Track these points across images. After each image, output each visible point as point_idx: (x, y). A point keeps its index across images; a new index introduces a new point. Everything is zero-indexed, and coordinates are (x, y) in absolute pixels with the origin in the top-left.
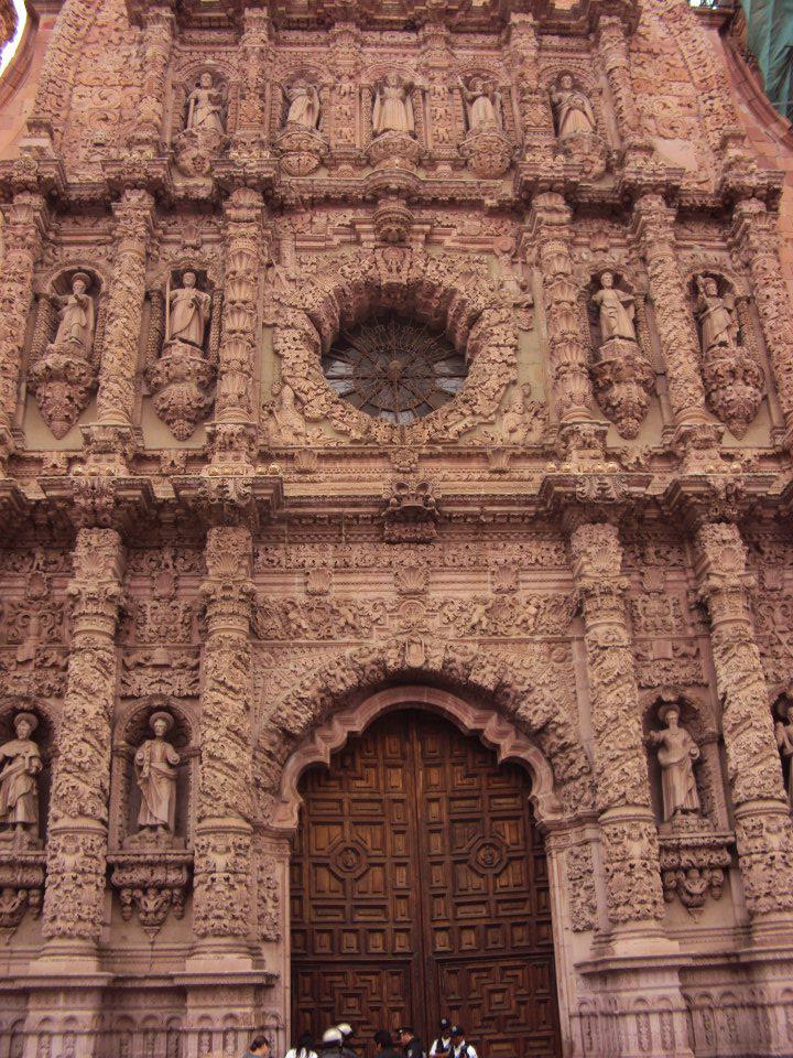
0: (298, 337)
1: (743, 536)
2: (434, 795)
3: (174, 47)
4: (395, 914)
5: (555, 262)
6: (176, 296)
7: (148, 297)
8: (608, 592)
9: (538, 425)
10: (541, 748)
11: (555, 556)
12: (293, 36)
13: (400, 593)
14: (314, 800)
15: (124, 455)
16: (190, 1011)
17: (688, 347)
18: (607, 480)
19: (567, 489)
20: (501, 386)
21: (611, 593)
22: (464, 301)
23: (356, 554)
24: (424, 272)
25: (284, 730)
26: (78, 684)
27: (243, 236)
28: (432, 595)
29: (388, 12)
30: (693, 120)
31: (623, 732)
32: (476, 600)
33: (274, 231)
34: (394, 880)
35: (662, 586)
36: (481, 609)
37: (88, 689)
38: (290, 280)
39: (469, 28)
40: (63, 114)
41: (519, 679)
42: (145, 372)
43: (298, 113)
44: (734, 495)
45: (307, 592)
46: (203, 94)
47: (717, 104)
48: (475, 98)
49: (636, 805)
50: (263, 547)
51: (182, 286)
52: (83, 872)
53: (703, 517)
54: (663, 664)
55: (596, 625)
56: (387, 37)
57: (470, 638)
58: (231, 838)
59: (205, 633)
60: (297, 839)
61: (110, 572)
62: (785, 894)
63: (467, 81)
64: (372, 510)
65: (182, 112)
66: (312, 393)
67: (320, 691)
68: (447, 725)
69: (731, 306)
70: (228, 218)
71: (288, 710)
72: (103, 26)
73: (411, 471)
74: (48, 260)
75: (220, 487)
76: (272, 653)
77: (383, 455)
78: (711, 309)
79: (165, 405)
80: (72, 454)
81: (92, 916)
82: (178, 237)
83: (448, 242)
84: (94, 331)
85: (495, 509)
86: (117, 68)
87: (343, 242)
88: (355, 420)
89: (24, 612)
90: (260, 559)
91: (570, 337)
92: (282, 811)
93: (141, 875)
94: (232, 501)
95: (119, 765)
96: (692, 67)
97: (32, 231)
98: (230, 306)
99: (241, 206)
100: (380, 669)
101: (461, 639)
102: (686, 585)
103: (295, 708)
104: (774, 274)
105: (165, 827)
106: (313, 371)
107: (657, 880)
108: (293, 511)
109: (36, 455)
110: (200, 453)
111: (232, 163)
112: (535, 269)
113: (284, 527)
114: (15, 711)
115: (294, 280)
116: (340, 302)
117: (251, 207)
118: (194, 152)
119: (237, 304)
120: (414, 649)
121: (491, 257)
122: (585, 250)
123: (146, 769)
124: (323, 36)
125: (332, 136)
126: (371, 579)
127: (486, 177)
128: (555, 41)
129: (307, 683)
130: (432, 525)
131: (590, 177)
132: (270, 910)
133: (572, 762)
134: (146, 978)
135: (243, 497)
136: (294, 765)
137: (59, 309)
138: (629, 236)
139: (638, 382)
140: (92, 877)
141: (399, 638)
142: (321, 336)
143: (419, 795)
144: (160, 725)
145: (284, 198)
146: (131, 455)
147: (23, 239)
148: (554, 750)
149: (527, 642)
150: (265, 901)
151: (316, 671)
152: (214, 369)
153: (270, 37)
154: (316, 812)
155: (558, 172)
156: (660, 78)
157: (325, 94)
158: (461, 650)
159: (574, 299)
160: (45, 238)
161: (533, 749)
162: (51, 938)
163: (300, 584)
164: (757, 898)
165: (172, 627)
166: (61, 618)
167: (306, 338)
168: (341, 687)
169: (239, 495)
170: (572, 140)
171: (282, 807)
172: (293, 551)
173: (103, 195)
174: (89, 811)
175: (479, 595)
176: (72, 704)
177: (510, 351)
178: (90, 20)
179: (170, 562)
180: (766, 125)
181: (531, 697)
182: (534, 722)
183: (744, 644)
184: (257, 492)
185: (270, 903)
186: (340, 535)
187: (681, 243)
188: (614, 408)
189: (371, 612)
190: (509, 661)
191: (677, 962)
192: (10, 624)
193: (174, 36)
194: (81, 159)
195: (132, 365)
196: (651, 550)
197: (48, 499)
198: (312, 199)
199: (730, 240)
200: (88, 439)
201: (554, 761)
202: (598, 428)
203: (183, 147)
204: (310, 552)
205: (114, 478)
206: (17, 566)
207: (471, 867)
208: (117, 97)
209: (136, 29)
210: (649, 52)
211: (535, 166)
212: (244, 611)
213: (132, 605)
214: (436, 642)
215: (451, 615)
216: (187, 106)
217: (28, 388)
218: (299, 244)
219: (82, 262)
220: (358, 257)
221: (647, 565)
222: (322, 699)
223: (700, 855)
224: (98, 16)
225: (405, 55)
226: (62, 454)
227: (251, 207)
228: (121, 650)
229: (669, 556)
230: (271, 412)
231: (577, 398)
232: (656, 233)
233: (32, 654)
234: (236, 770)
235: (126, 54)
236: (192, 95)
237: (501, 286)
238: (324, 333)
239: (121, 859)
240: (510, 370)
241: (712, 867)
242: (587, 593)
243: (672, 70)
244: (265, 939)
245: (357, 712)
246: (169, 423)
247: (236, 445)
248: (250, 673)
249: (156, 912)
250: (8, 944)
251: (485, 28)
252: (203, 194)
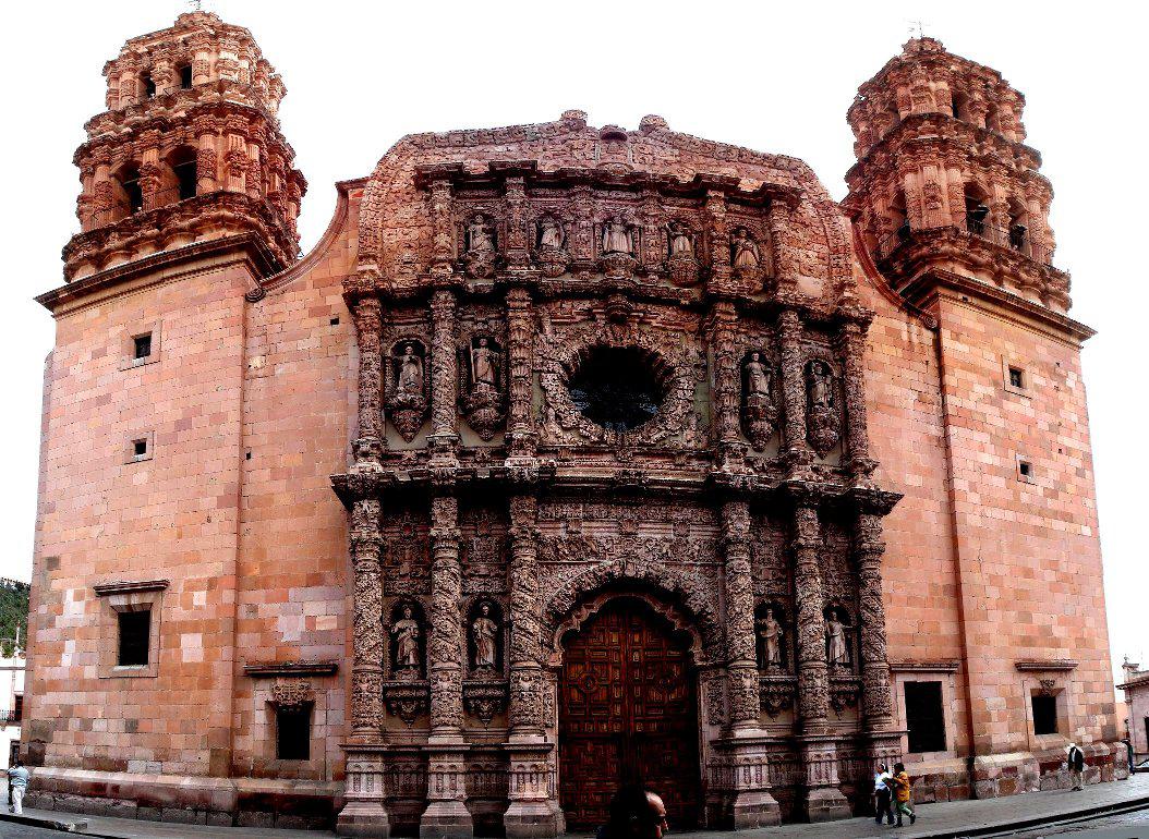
69: (828, 382)
244: (547, 726)
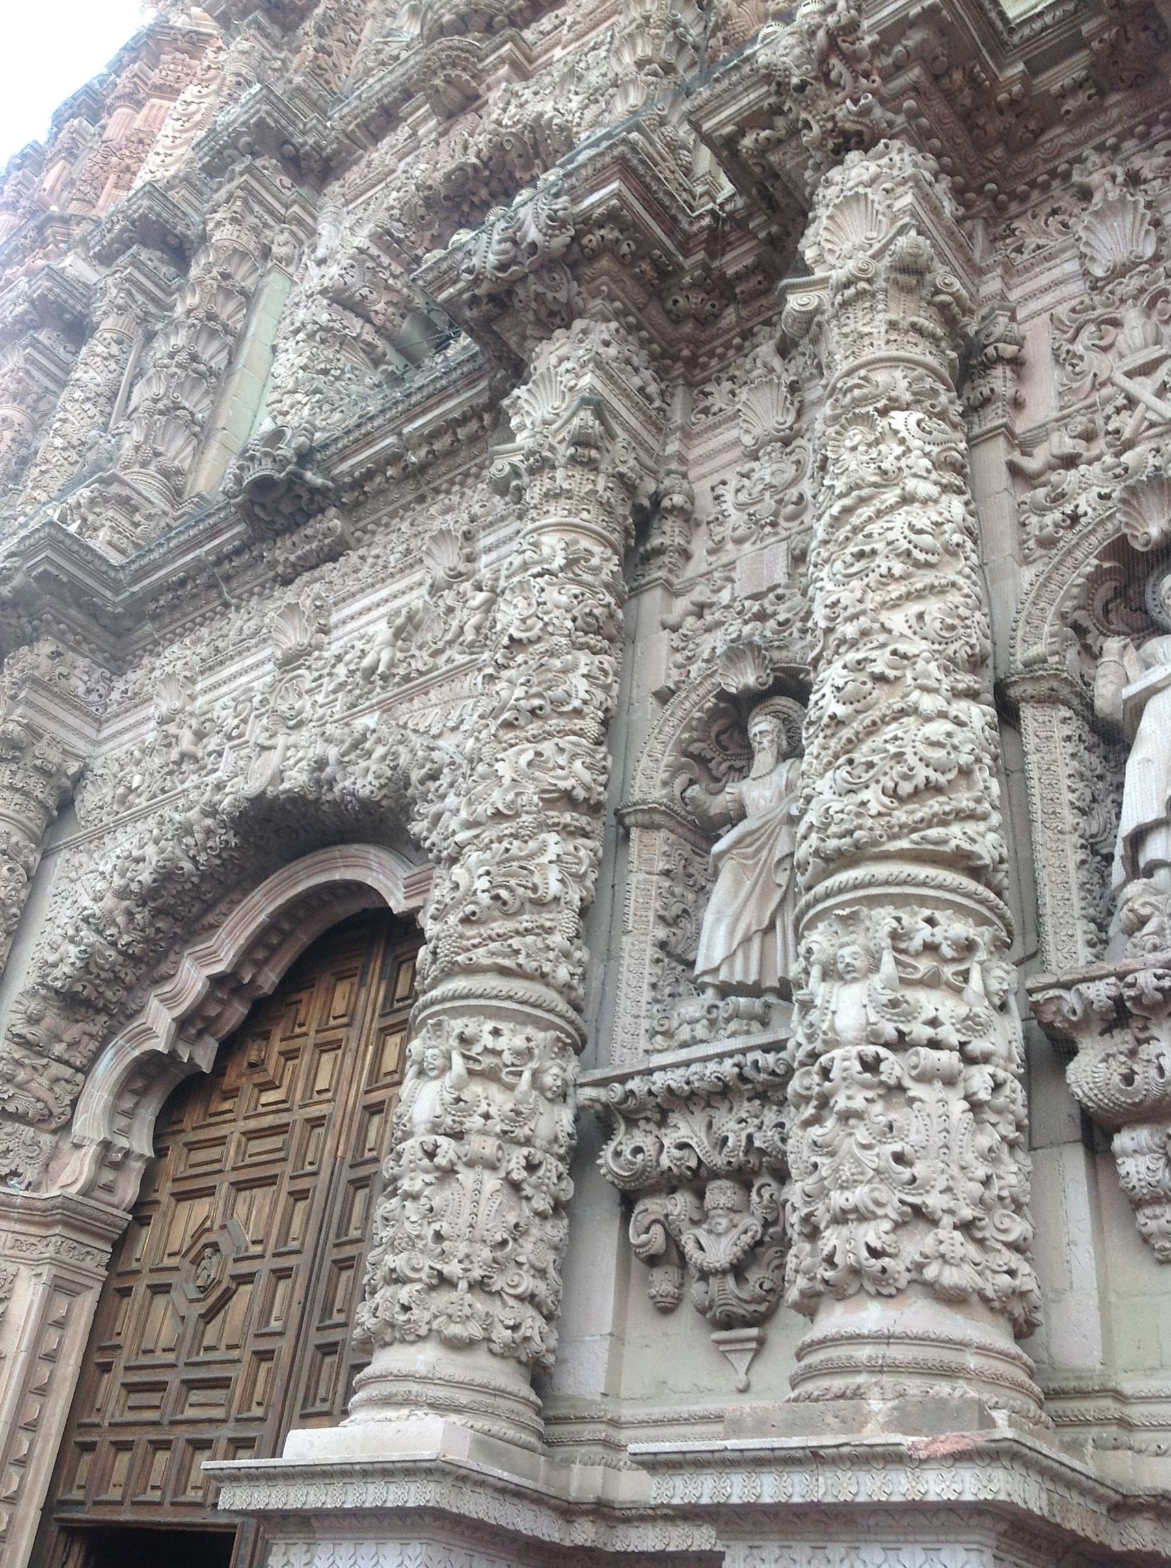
4: (246, 1404)
49: (471, 970)
113: (148, 627)
116: (396, 256)
145: (317, 147)
198: (364, 126)
222: (130, 914)
223: (728, 1124)
245: (221, 933)
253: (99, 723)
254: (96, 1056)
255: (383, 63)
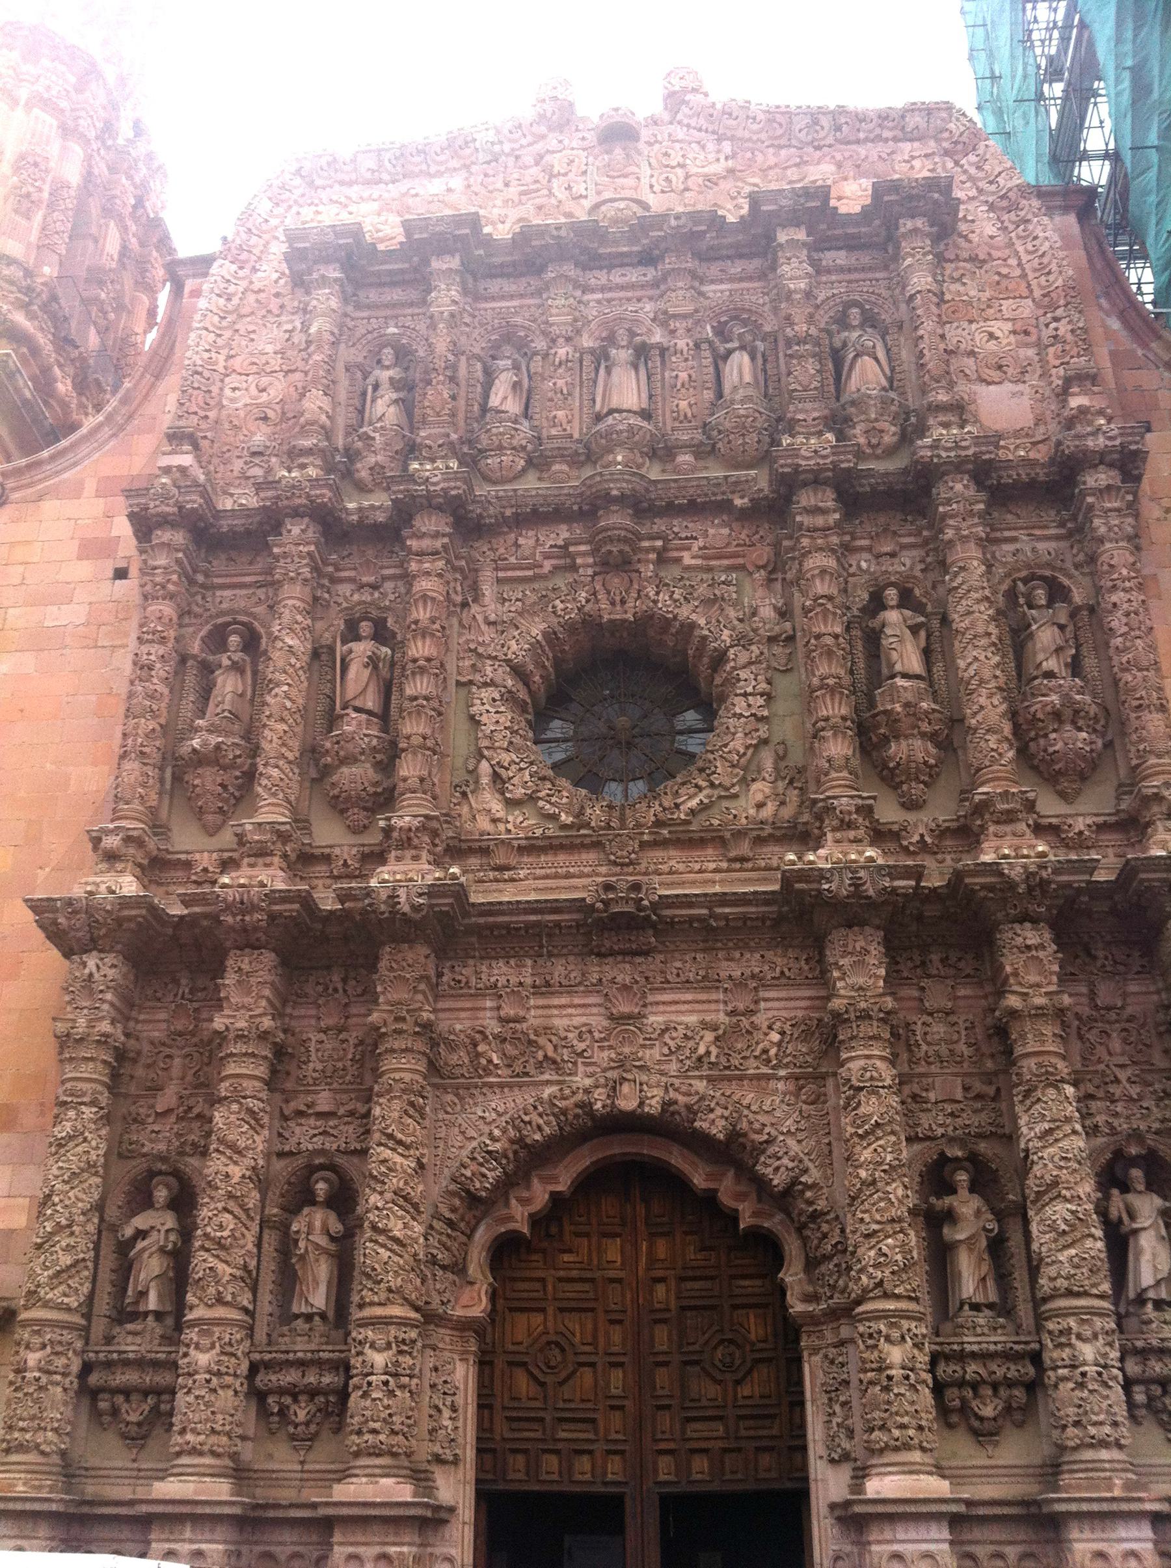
0: (497, 697)
1: (1057, 940)
2: (660, 1274)
3: (346, 315)
4: (607, 1431)
5: (818, 582)
6: (351, 651)
7: (316, 654)
8: (865, 1016)
9: (793, 795)
10: (789, 1215)
11: (806, 968)
12: (495, 286)
13: (611, 1017)
14: (514, 1279)
15: (285, 856)
16: (336, 1548)
17: (993, 684)
18: (862, 874)
19: (815, 886)
20: (747, 748)
21: (870, 1017)
22: (705, 638)
23: (559, 970)
24: (655, 602)
25: (468, 1192)
26: (221, 1141)
27: (428, 574)
28: (652, 1019)
29: (616, 243)
30: (1031, 352)
31: (881, 1199)
32: (705, 1025)
33: (470, 560)
34: (608, 1384)
35: (950, 1005)
36: (709, 1036)
37: (233, 1147)
38: (490, 624)
39: (725, 252)
40: (212, 414)
41: (757, 1126)
42: (313, 750)
43: (500, 395)
44: (1037, 885)
45: (501, 1019)
46: (384, 375)
47: (1063, 328)
48: (730, 352)
50: (448, 964)
51: (358, 638)
52: (219, 1374)
53: (1000, 916)
54: (949, 1108)
55: (851, 1059)
56: (616, 277)
57: (697, 1073)
58: (393, 1330)
59: (377, 1074)
60: (489, 1329)
61: (264, 1003)
62: (1101, 1423)
63: (721, 332)
64: (575, 916)
65: (357, 402)
66: (514, 767)
67: (512, 1142)
68: (677, 1183)
70: (409, 550)
71: (474, 1167)
72: (260, 291)
73: (631, 863)
74: (196, 609)
75: (389, 897)
76: (457, 1095)
77: (597, 845)
78: (1034, 627)
79: (336, 792)
80: (226, 855)
81: (227, 1428)
82: (352, 574)
83: (688, 560)
84: (252, 700)
85: (727, 910)
86: (278, 347)
87: (556, 568)
88: (565, 800)
89: (167, 1051)
90: (445, 979)
91: (831, 681)
92: (467, 1295)
93: (290, 1377)
94: (404, 914)
95: (271, 1240)
96: (1031, 276)
97: (175, 577)
98: (410, 665)
99: (424, 535)
100: (585, 1113)
101: (684, 1075)
102: (983, 1002)
103: (481, 1165)
104: (1125, 572)
105: (323, 1316)
106: (517, 740)
107: (926, 1396)
108: (482, 920)
109: (183, 857)
110: (377, 849)
111: (411, 478)
112: (795, 589)
113: (474, 939)
114: (152, 1174)
115: (494, 623)
117: (436, 535)
118: (372, 460)
119: (422, 663)
120: (626, 1088)
121: (742, 575)
122: (866, 555)
123: (302, 1244)
124: (535, 282)
125: (545, 424)
126: (577, 1001)
127: (737, 467)
128: (840, 258)
129: (497, 1132)
130: (651, 932)
131: (879, 451)
132: (447, 1423)
133: (825, 1236)
134: (291, 1506)
135: (416, 908)
136: (483, 1235)
137: (213, 672)
138: (925, 533)
139: (923, 735)
140: (229, 1380)
141: (609, 1074)
142: (530, 691)
143: (640, 1273)
144: (321, 1187)
145: (480, 516)
146: (293, 856)
147: (163, 587)
148: (803, 1219)
149: (768, 1077)
150: (439, 1411)
151: (507, 1117)
152: (394, 744)
153: (465, 292)
154: (515, 1295)
155: (824, 457)
156: (988, 294)
157: (537, 364)
158: (684, 1088)
159: (838, 630)
160: (192, 582)
161: (779, 1217)
162: (178, 1454)
163: (491, 1009)
164: (1064, 1427)
165: (340, 1065)
166: (210, 1057)
167: (509, 697)
168: (537, 1137)
169: (413, 907)
170: (853, 403)
171: (469, 1288)
172: (484, 968)
173: (261, 523)
174: (229, 1298)
175: (708, 1019)
176: (216, 1164)
177: (761, 701)
178: (244, 284)
179: (340, 986)
180: (1145, 345)
181: (771, 1150)
182: (775, 1182)
183: (1051, 1085)
184: (434, 901)
185: (447, 1413)
186: (541, 947)
187: (998, 534)
188: (892, 770)
189: (575, 1042)
190: (745, 1102)
191: (944, 1508)
192: (149, 1066)
193: (346, 300)
194: (236, 474)
195: (295, 744)
196: (935, 957)
197: (189, 915)
198: (516, 514)
199: (1069, 525)
200: (241, 839)
201: (808, 1233)
202: (860, 802)
203: (358, 452)
204: (504, 969)
205: (267, 890)
206: (159, 995)
207: (703, 1369)
208: (278, 388)
209: (300, 292)
210: (973, 259)
211: (793, 452)
212: (420, 1045)
213: (291, 1040)
214: (654, 1079)
215: (672, 1043)
216: (364, 394)
217: (173, 774)
218: (501, 574)
219: (237, 613)
220: (574, 587)
221: (929, 976)
222: (515, 1152)
224: (255, 278)
225: (639, 300)
226: (215, 856)
227: (436, 535)
228: (278, 1096)
229: (962, 965)
230: (464, 794)
231: (836, 763)
232: (958, 529)
233: (173, 1102)
234: (404, 1246)
235: (289, 327)
236: (371, 380)
237: (754, 614)
238: (534, 687)
239: (267, 1357)
240: (760, 726)
241: (1010, 1384)
242: (839, 1018)
243: (1004, 283)
244: (438, 1460)
246: (343, 812)
247: (416, 841)
248: (427, 1123)
249: (307, 1424)
250: (134, 1461)
251: (746, 251)
252: (381, 517)
253: (437, 997)
254: (473, 1230)
255: (514, 448)
